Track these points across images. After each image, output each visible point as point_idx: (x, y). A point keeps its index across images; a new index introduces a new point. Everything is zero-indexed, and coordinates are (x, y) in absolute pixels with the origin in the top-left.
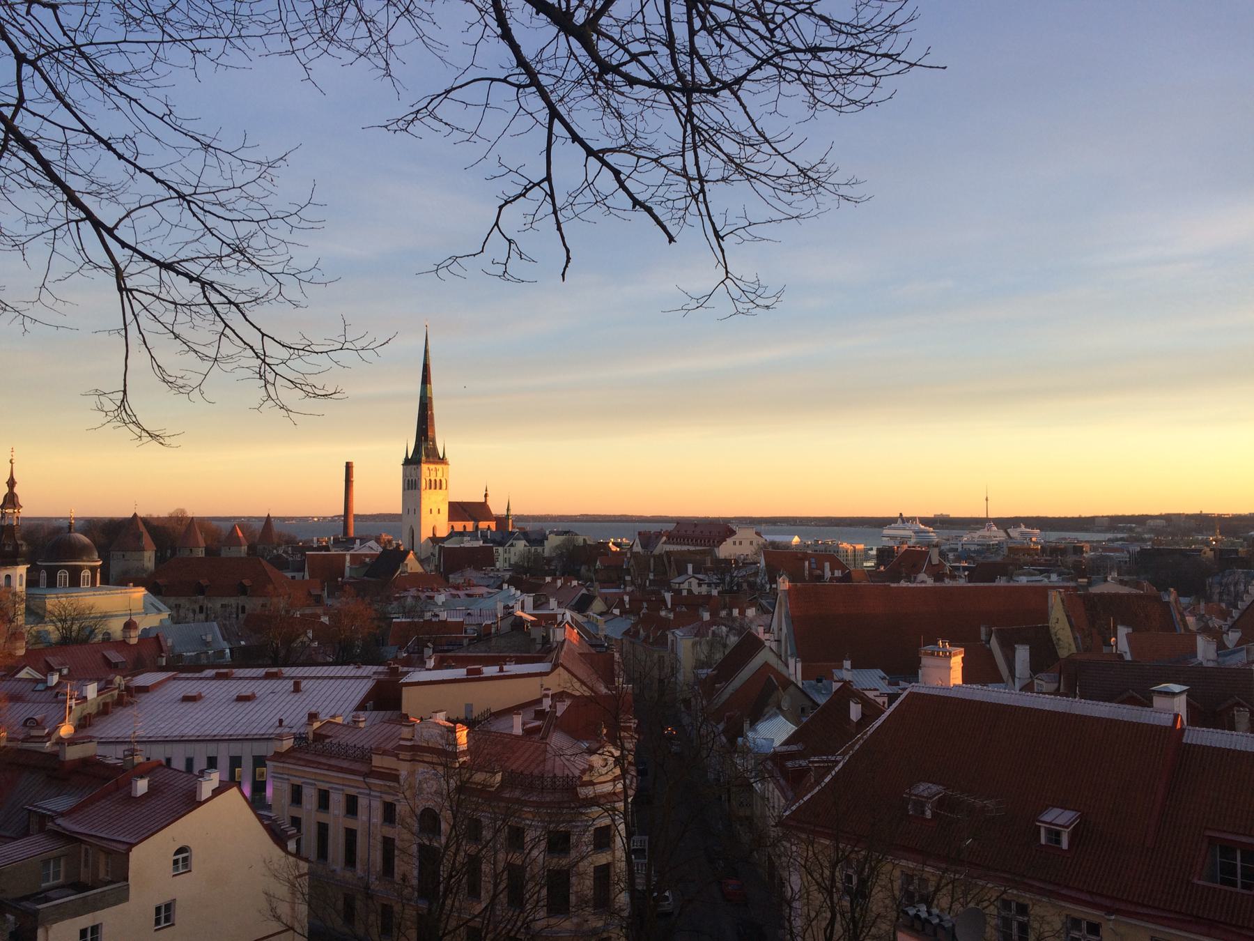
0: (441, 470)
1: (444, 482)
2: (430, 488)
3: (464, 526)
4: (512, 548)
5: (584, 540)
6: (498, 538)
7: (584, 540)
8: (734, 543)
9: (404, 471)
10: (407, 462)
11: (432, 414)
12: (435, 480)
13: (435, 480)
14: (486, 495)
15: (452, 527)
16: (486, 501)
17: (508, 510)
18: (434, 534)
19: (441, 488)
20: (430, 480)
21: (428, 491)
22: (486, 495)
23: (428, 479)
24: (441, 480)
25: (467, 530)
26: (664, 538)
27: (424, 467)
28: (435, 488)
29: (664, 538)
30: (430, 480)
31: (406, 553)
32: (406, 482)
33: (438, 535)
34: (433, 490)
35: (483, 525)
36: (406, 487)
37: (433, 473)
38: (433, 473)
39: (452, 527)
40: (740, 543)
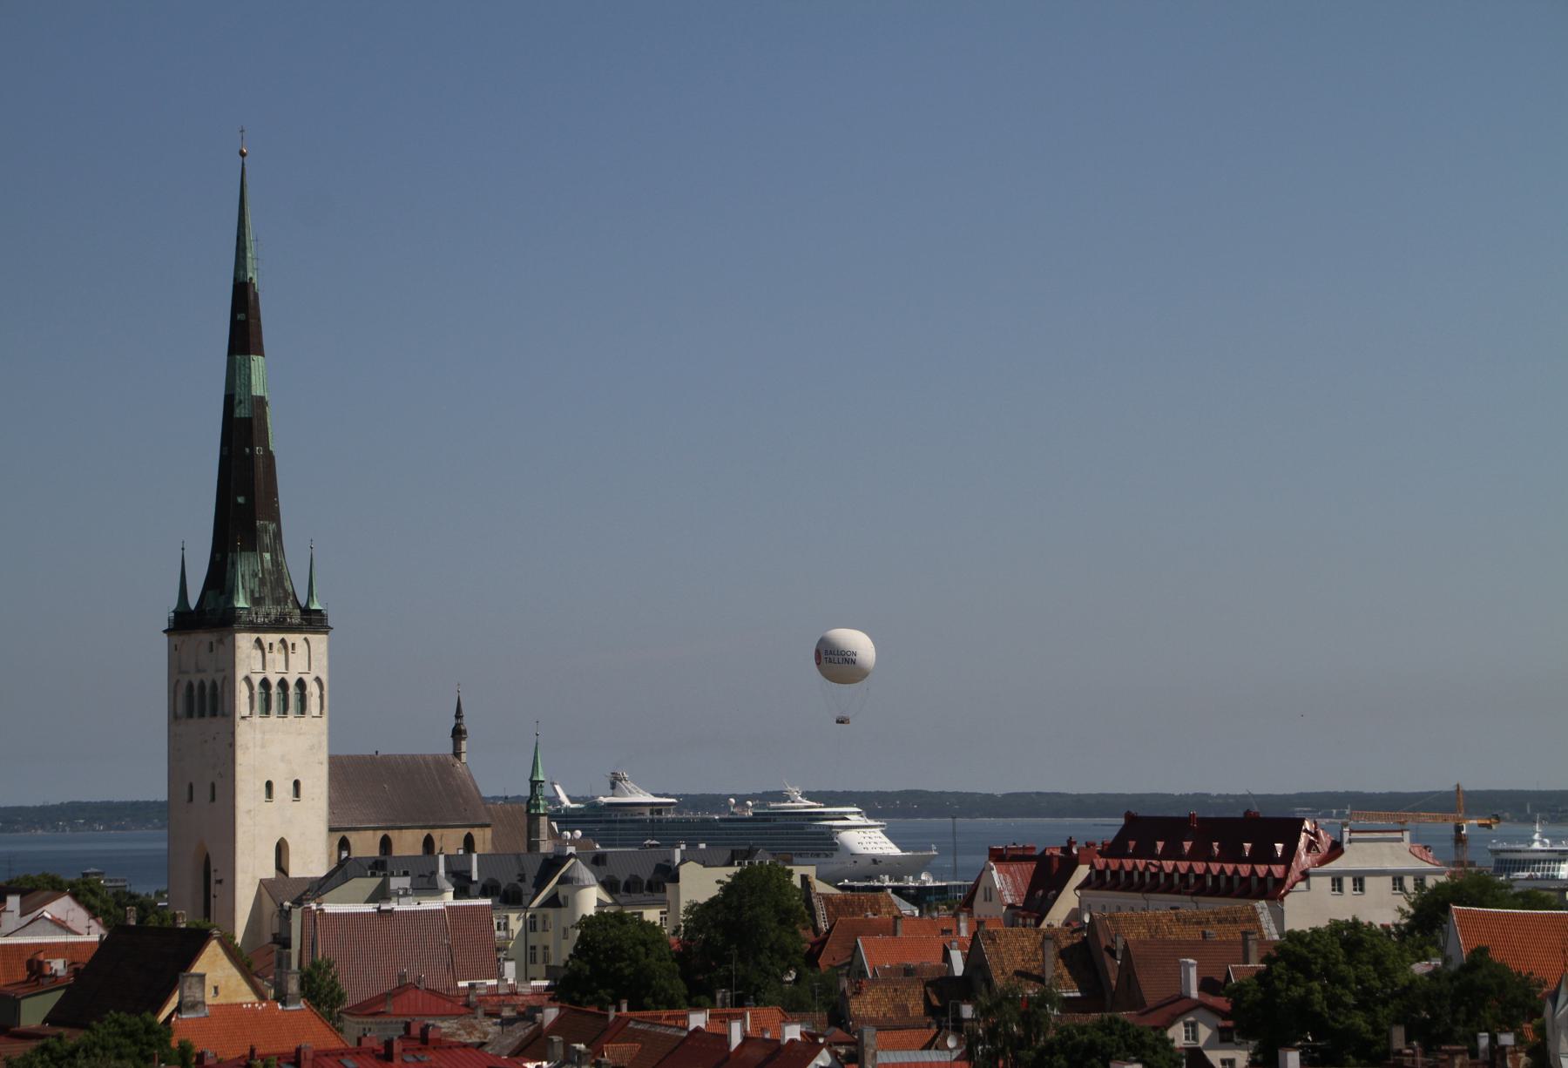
0: (301, 648)
1: (312, 689)
2: (267, 710)
3: (386, 844)
4: (551, 912)
5: (804, 878)
6: (506, 880)
7: (804, 878)
8: (1337, 883)
9: (174, 650)
10: (184, 622)
11: (269, 457)
12: (283, 684)
13: (283, 684)
14: (458, 733)
15: (344, 844)
16: (457, 754)
17: (534, 784)
18: (281, 867)
19: (303, 709)
20: (265, 683)
21: (256, 719)
22: (458, 733)
23: (256, 680)
24: (301, 684)
25: (396, 852)
26: (1082, 872)
27: (244, 642)
28: (285, 710)
29: (1082, 872)
30: (265, 683)
31: (195, 941)
32: (182, 690)
33: (295, 871)
34: (273, 718)
35: (449, 841)
36: (181, 708)
37: (277, 658)
38: (277, 658)
39: (344, 844)
40: (1359, 883)
